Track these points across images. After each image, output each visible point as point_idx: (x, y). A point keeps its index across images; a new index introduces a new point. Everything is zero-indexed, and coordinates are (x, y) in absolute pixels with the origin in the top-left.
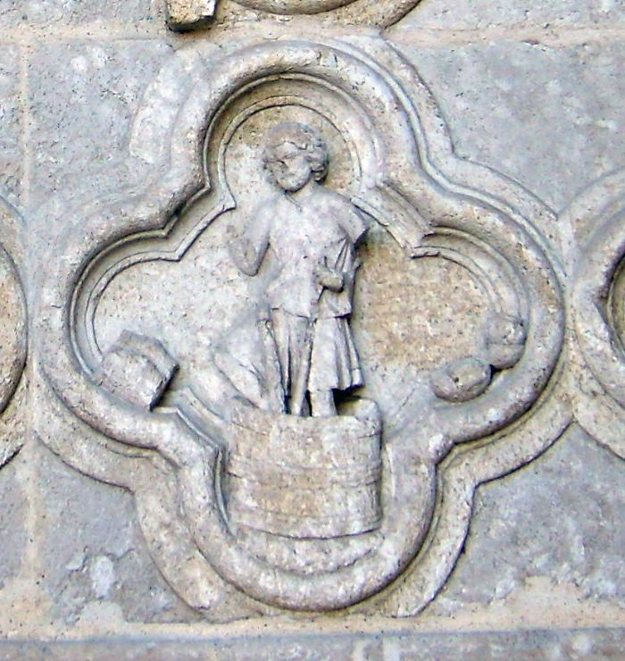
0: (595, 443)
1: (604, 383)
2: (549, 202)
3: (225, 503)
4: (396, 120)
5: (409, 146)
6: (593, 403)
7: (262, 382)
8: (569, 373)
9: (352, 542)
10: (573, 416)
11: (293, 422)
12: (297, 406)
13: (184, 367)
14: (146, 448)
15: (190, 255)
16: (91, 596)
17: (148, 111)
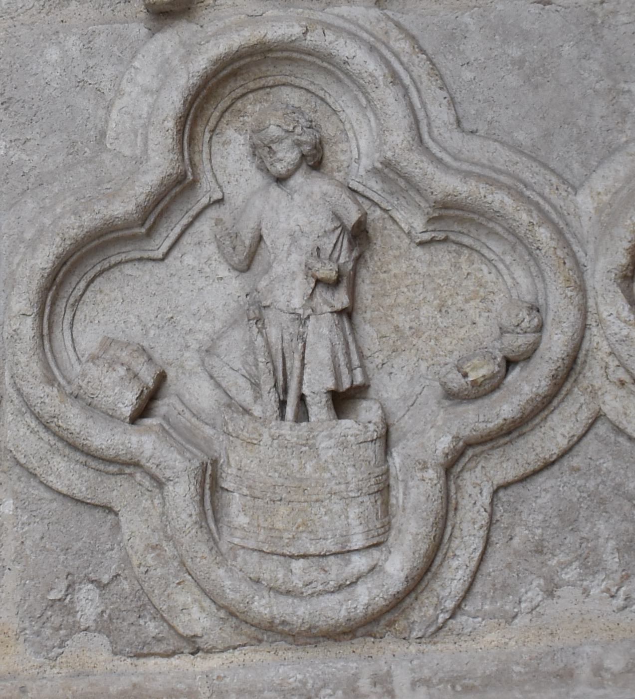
0: (626, 437)
1: (632, 371)
2: (567, 175)
3: (216, 521)
4: (388, 96)
5: (405, 123)
6: (621, 393)
7: (256, 386)
8: (593, 362)
9: (355, 558)
10: (600, 409)
11: (288, 430)
12: (290, 411)
13: (171, 374)
14: (127, 464)
15: (175, 253)
16: (75, 628)
17: (125, 100)
